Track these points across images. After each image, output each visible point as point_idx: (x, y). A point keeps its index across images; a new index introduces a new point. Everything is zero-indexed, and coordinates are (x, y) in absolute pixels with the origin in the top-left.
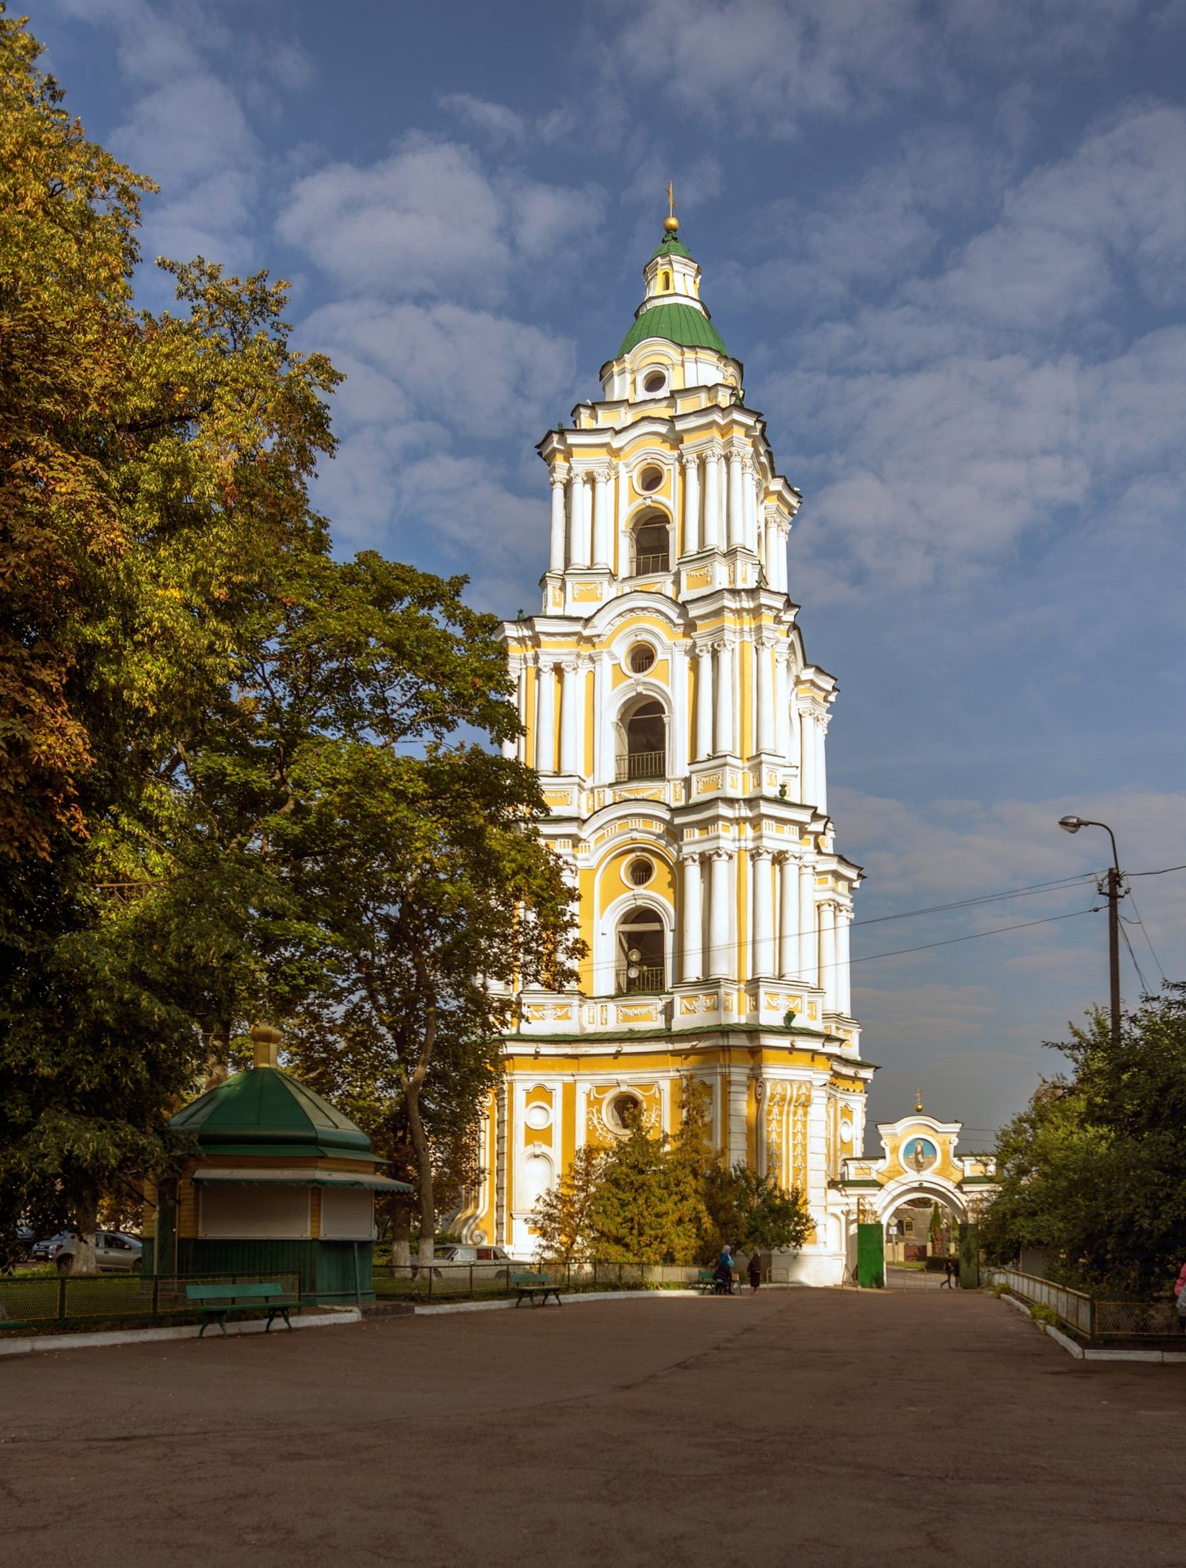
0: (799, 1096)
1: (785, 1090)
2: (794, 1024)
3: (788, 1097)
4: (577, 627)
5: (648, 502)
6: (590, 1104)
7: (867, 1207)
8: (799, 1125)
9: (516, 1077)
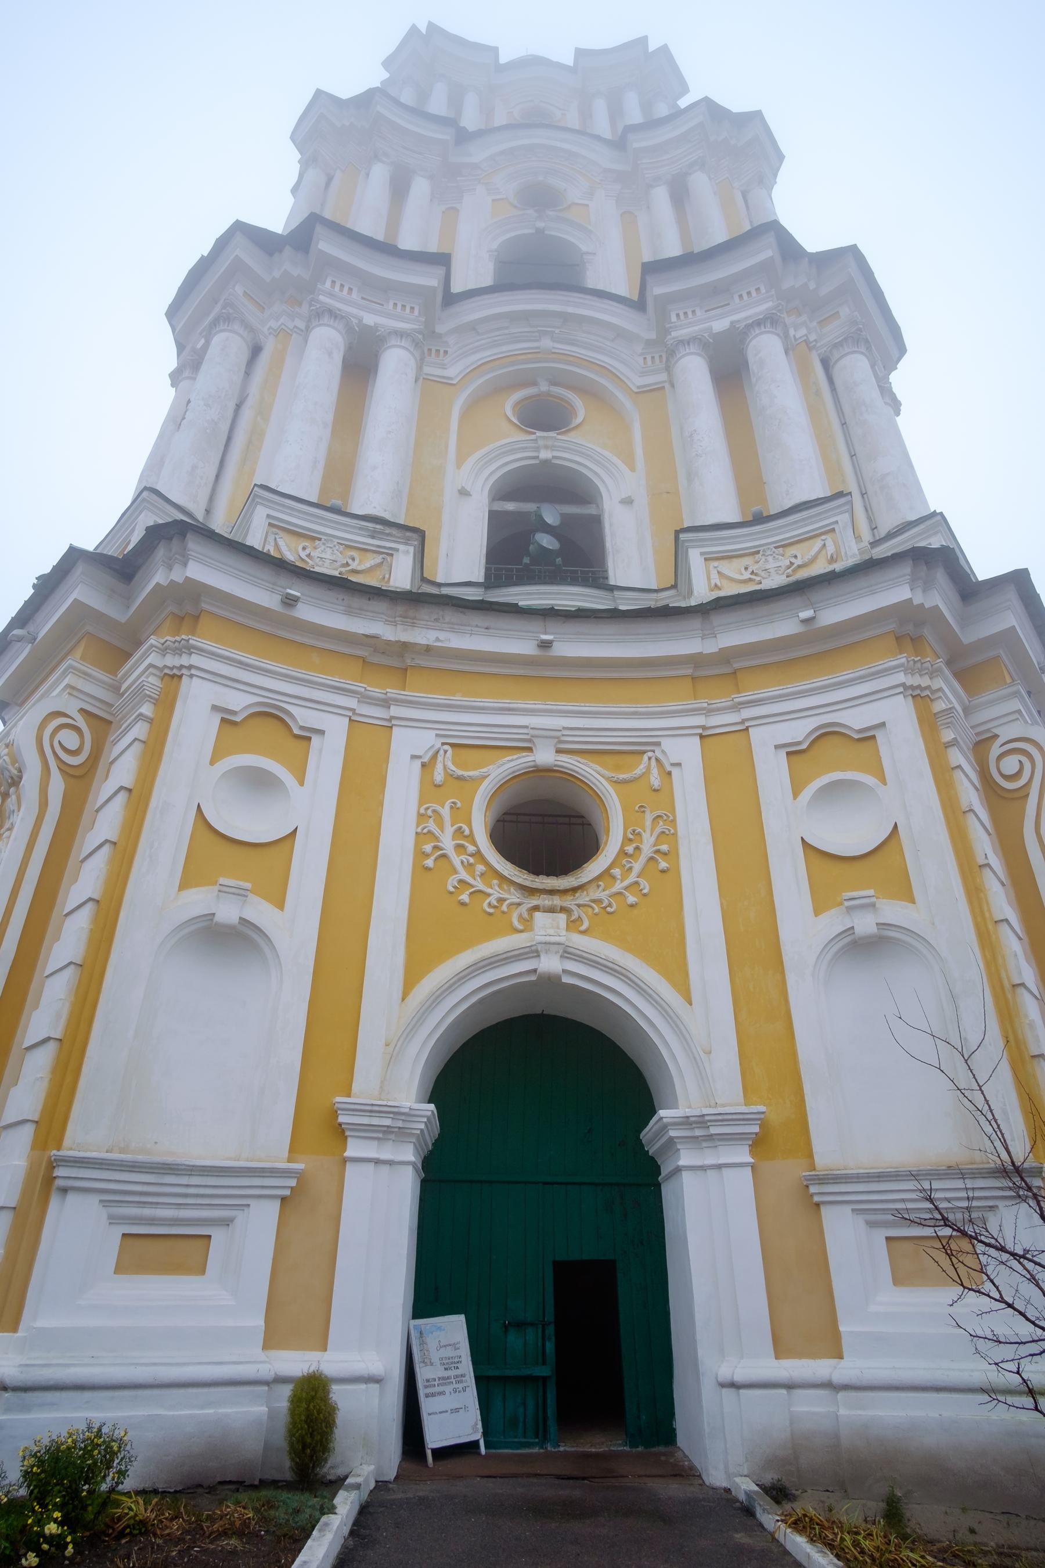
6: (430, 789)
9: (195, 660)
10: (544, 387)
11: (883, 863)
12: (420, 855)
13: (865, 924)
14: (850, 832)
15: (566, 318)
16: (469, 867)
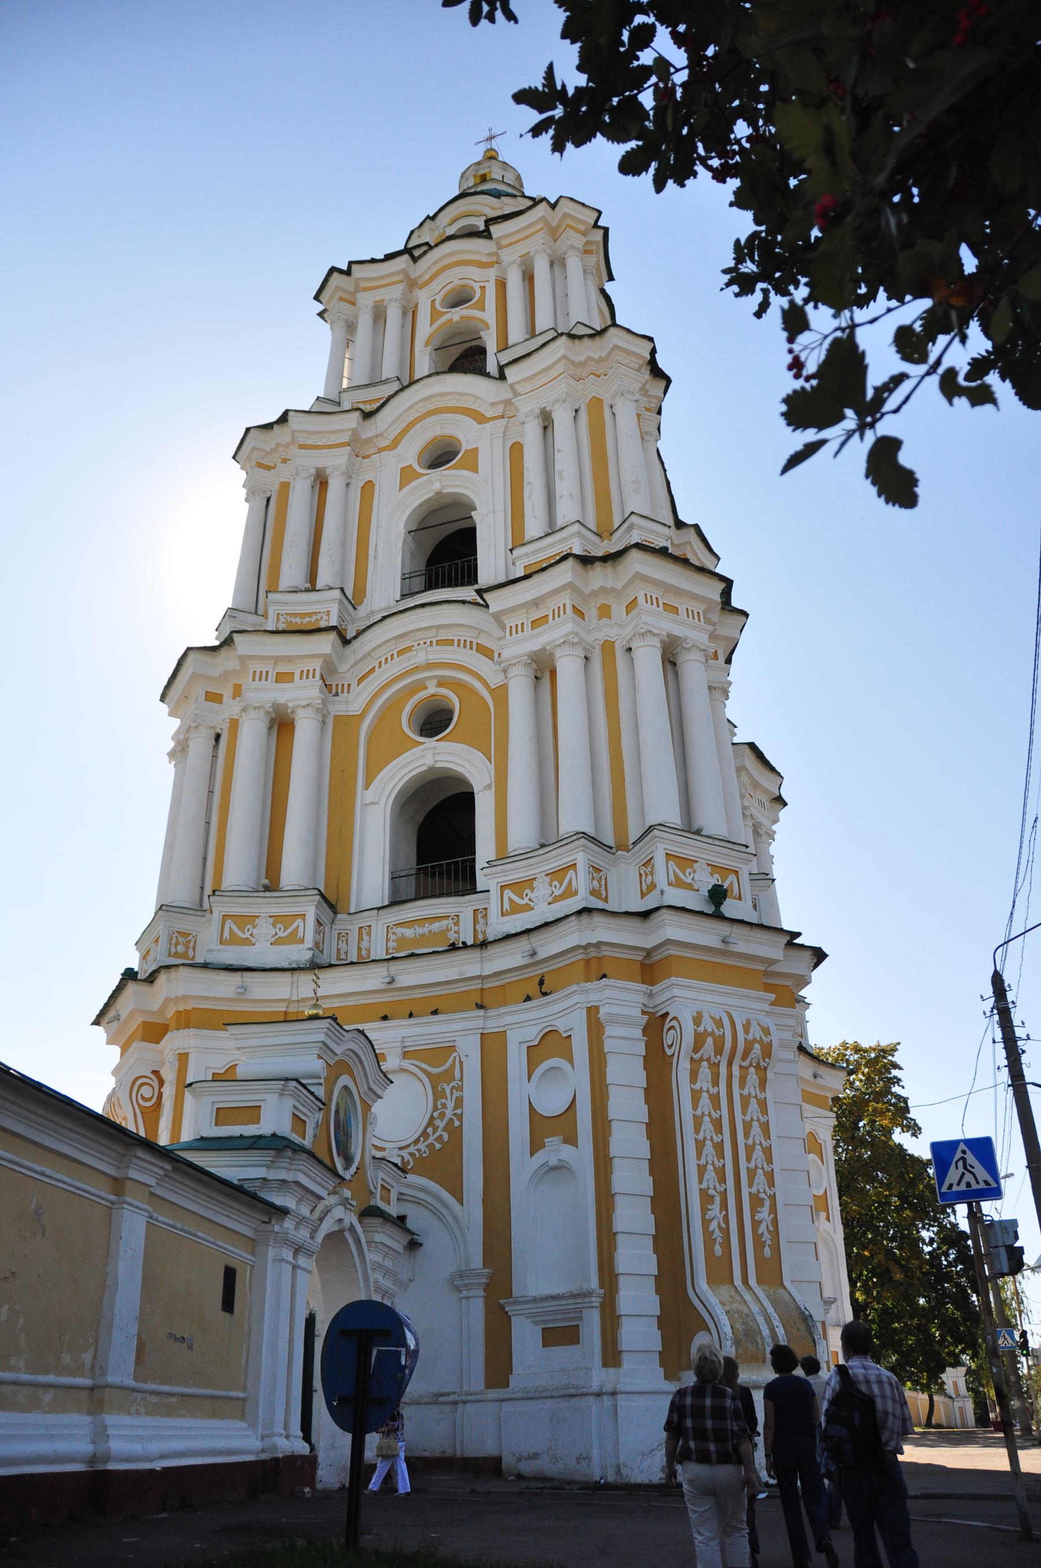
2: (729, 908)
10: (432, 689)
11: (563, 1125)
13: (554, 1162)
14: (552, 1104)
15: (439, 627)
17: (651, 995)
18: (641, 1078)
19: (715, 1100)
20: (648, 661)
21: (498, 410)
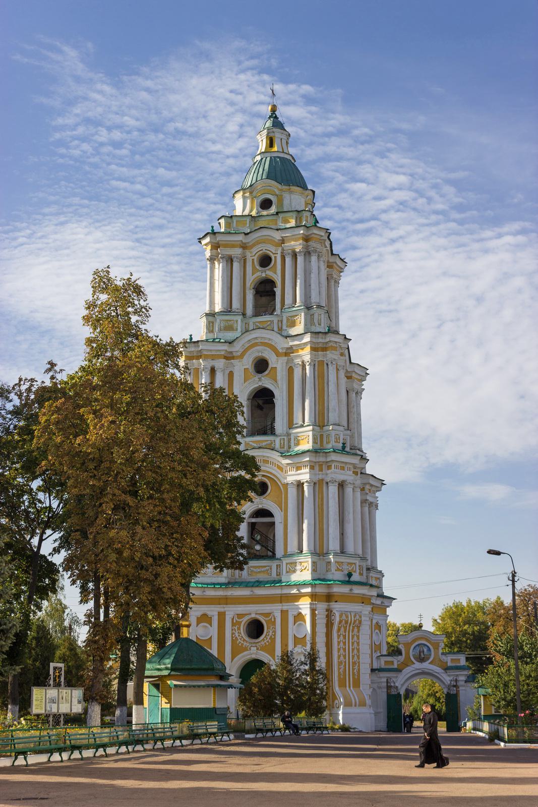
0: (355, 621)
1: (347, 617)
2: (352, 579)
3: (349, 621)
4: (226, 347)
5: (264, 275)
6: (233, 624)
7: (392, 684)
8: (355, 637)
12: (232, 637)
16: (241, 639)
17: (329, 605)
18: (325, 630)
19: (345, 637)
20: (333, 490)
21: (284, 351)
